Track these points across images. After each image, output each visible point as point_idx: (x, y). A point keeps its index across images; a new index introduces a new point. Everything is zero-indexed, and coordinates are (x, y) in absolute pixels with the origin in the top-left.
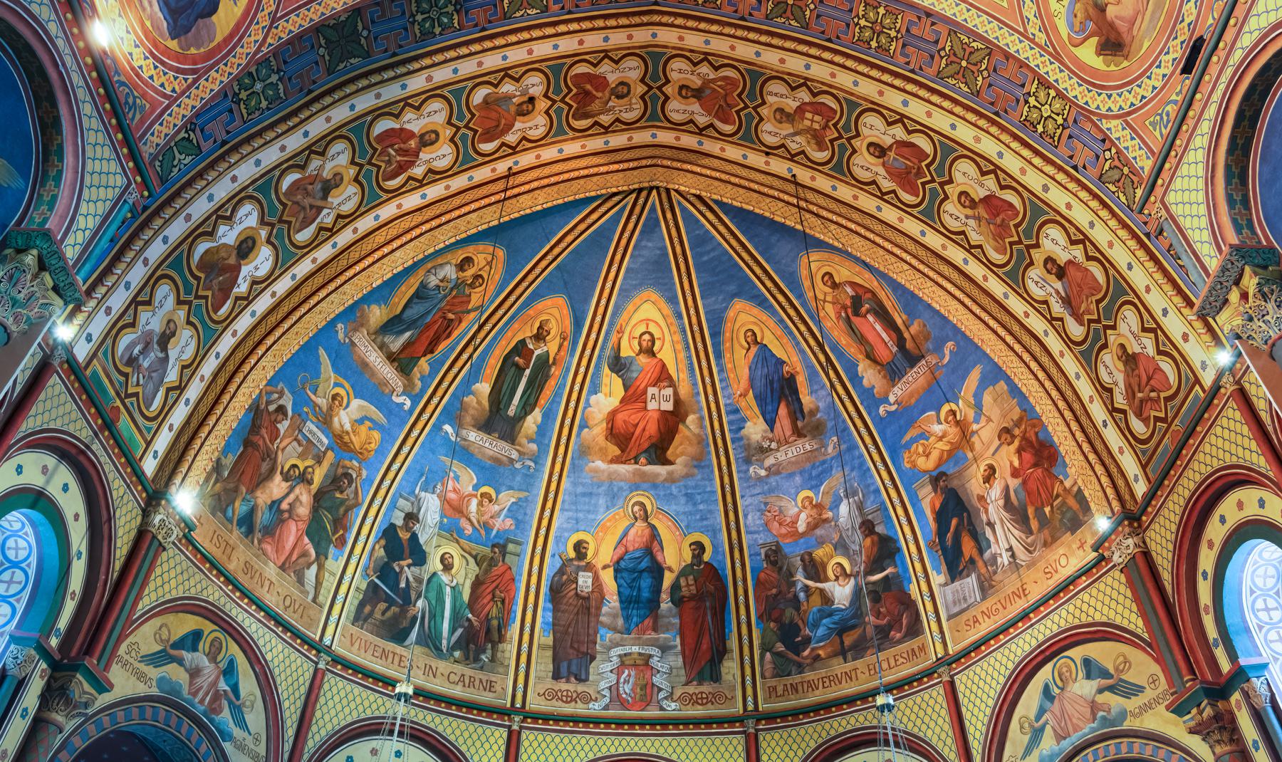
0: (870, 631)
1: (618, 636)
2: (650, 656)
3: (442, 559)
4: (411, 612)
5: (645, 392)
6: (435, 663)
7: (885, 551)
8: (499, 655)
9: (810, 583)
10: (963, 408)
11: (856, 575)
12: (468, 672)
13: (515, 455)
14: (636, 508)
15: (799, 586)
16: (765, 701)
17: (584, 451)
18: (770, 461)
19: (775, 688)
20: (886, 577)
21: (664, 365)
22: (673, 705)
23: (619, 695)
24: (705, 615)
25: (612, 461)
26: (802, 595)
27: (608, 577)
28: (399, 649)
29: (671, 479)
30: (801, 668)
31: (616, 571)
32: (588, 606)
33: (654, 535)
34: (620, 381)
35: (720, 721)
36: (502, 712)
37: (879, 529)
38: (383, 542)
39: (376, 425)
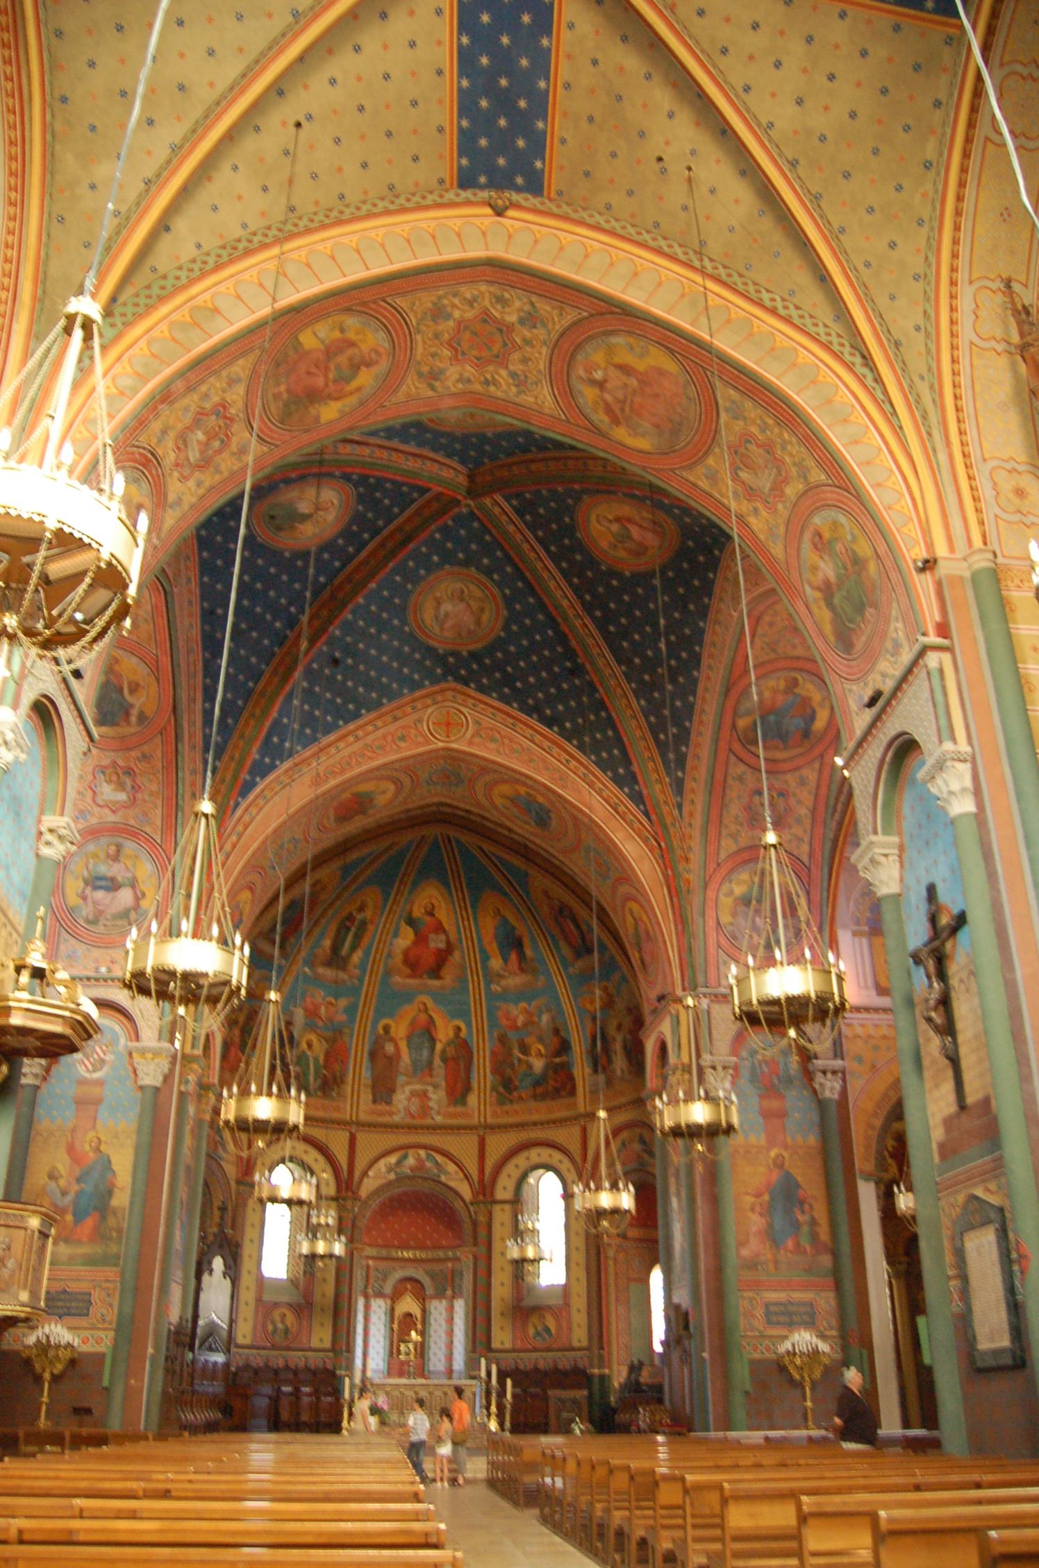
7: (564, 1047)
12: (326, 1102)
17: (388, 973)
18: (503, 983)
26: (516, 1062)
27: (403, 1045)
30: (511, 1102)
32: (393, 1061)
35: (465, 1128)
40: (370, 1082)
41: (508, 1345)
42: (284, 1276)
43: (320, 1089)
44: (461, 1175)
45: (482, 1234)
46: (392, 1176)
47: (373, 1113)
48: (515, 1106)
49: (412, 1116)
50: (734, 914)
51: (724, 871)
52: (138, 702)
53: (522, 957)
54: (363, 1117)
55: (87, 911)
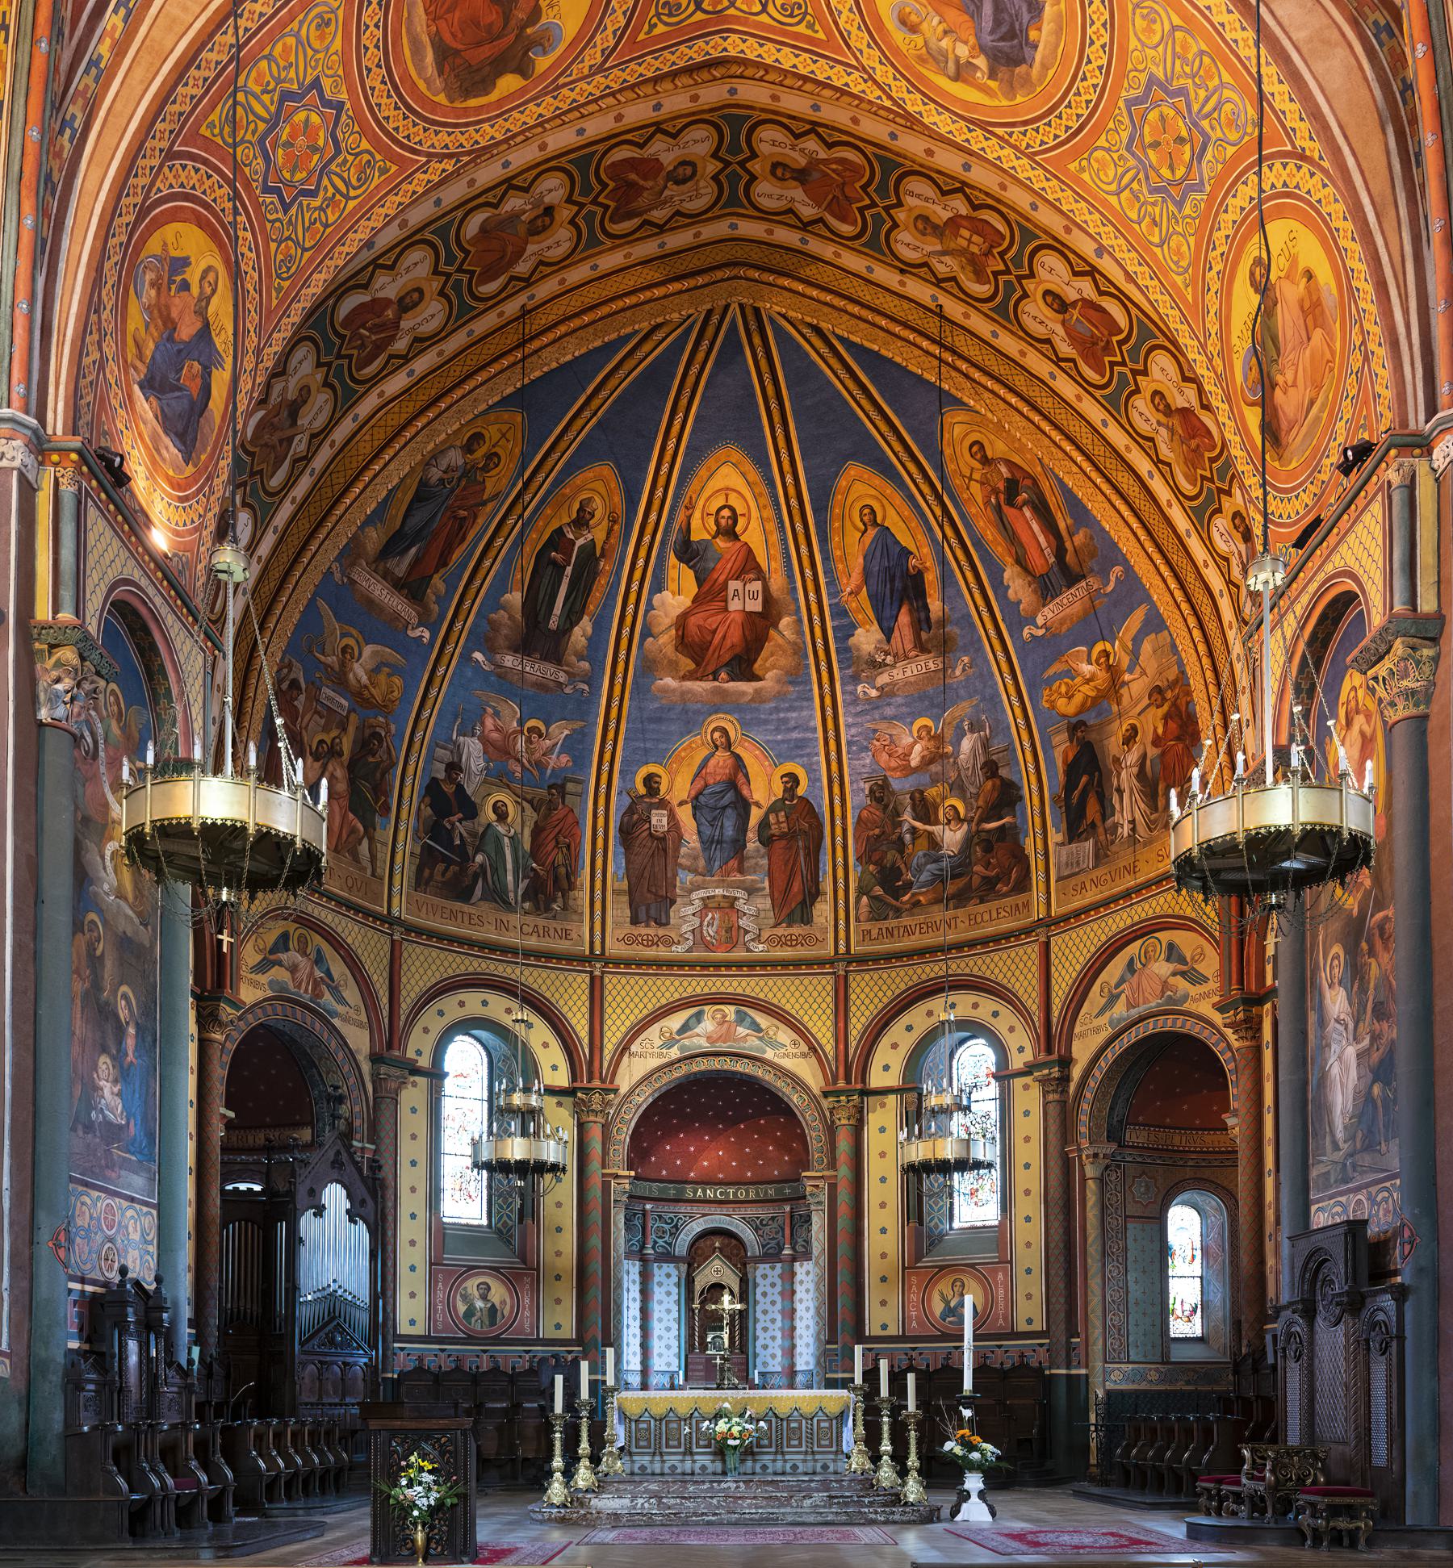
0: (976, 880)
1: (700, 878)
2: (736, 899)
4: (471, 871)
5: (725, 587)
6: (505, 917)
7: (1007, 797)
8: (571, 902)
9: (918, 824)
10: (1118, 650)
11: (970, 821)
12: (541, 922)
14: (717, 735)
16: (858, 944)
21: (750, 551)
22: (761, 947)
23: (702, 937)
24: (797, 854)
25: (684, 678)
26: (908, 837)
27: (685, 815)
28: (466, 908)
29: (758, 695)
30: (898, 913)
31: (694, 808)
32: (665, 845)
33: (739, 763)
34: (691, 573)
35: (809, 963)
36: (582, 960)
37: (1003, 772)
38: (428, 800)
39: (395, 670)
40: (625, 885)
47: (630, 940)
48: (906, 920)
54: (614, 948)
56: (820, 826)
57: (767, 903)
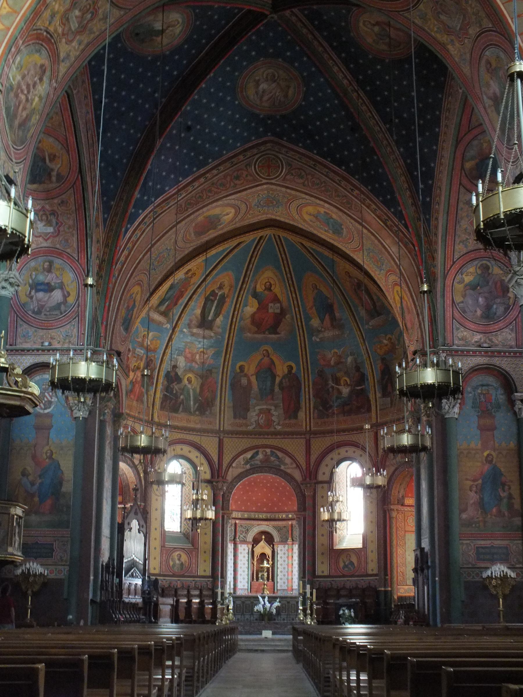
2: (271, 409)
3: (188, 380)
7: (362, 379)
13: (212, 334)
15: (330, 386)
16: (314, 427)
19: (318, 423)
20: (362, 389)
22: (280, 427)
23: (259, 424)
26: (331, 389)
27: (253, 379)
30: (328, 416)
40: (231, 405)
41: (326, 573)
42: (179, 531)
43: (198, 409)
44: (295, 465)
45: (309, 503)
46: (248, 467)
49: (261, 427)
50: (464, 296)
51: (457, 266)
52: (56, 167)
53: (333, 319)
55: (33, 306)
56: (301, 384)
57: (281, 411)
